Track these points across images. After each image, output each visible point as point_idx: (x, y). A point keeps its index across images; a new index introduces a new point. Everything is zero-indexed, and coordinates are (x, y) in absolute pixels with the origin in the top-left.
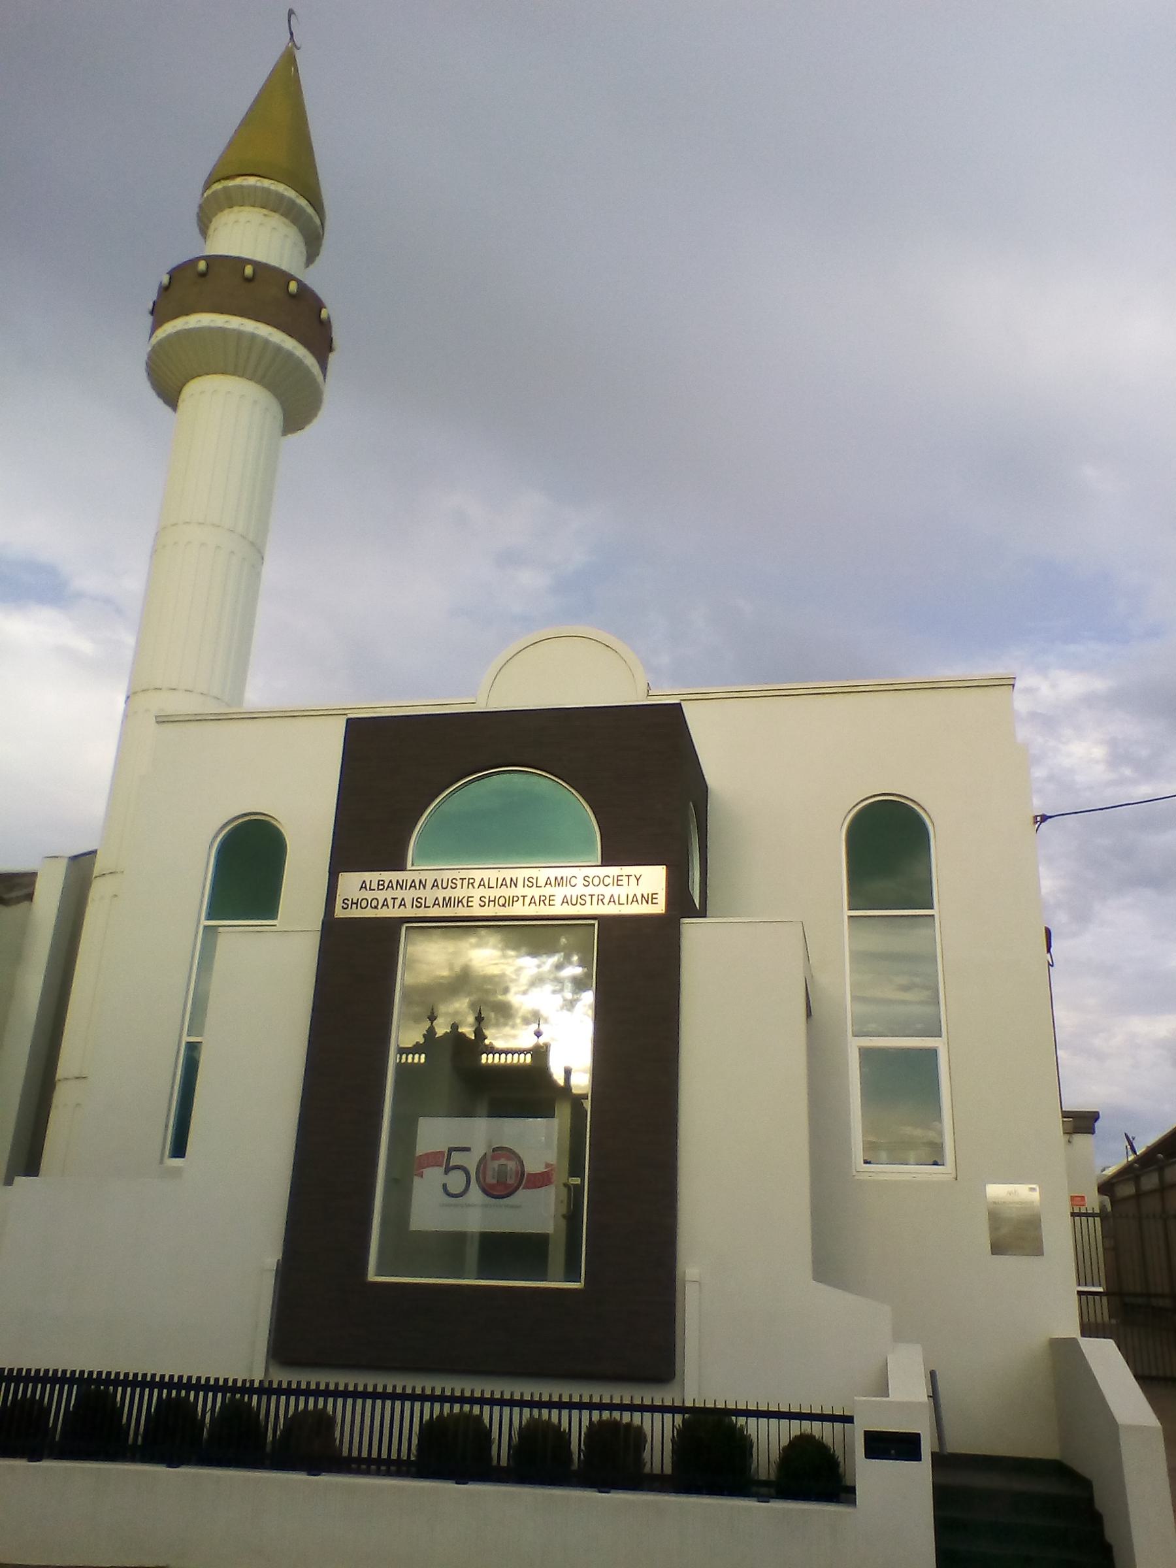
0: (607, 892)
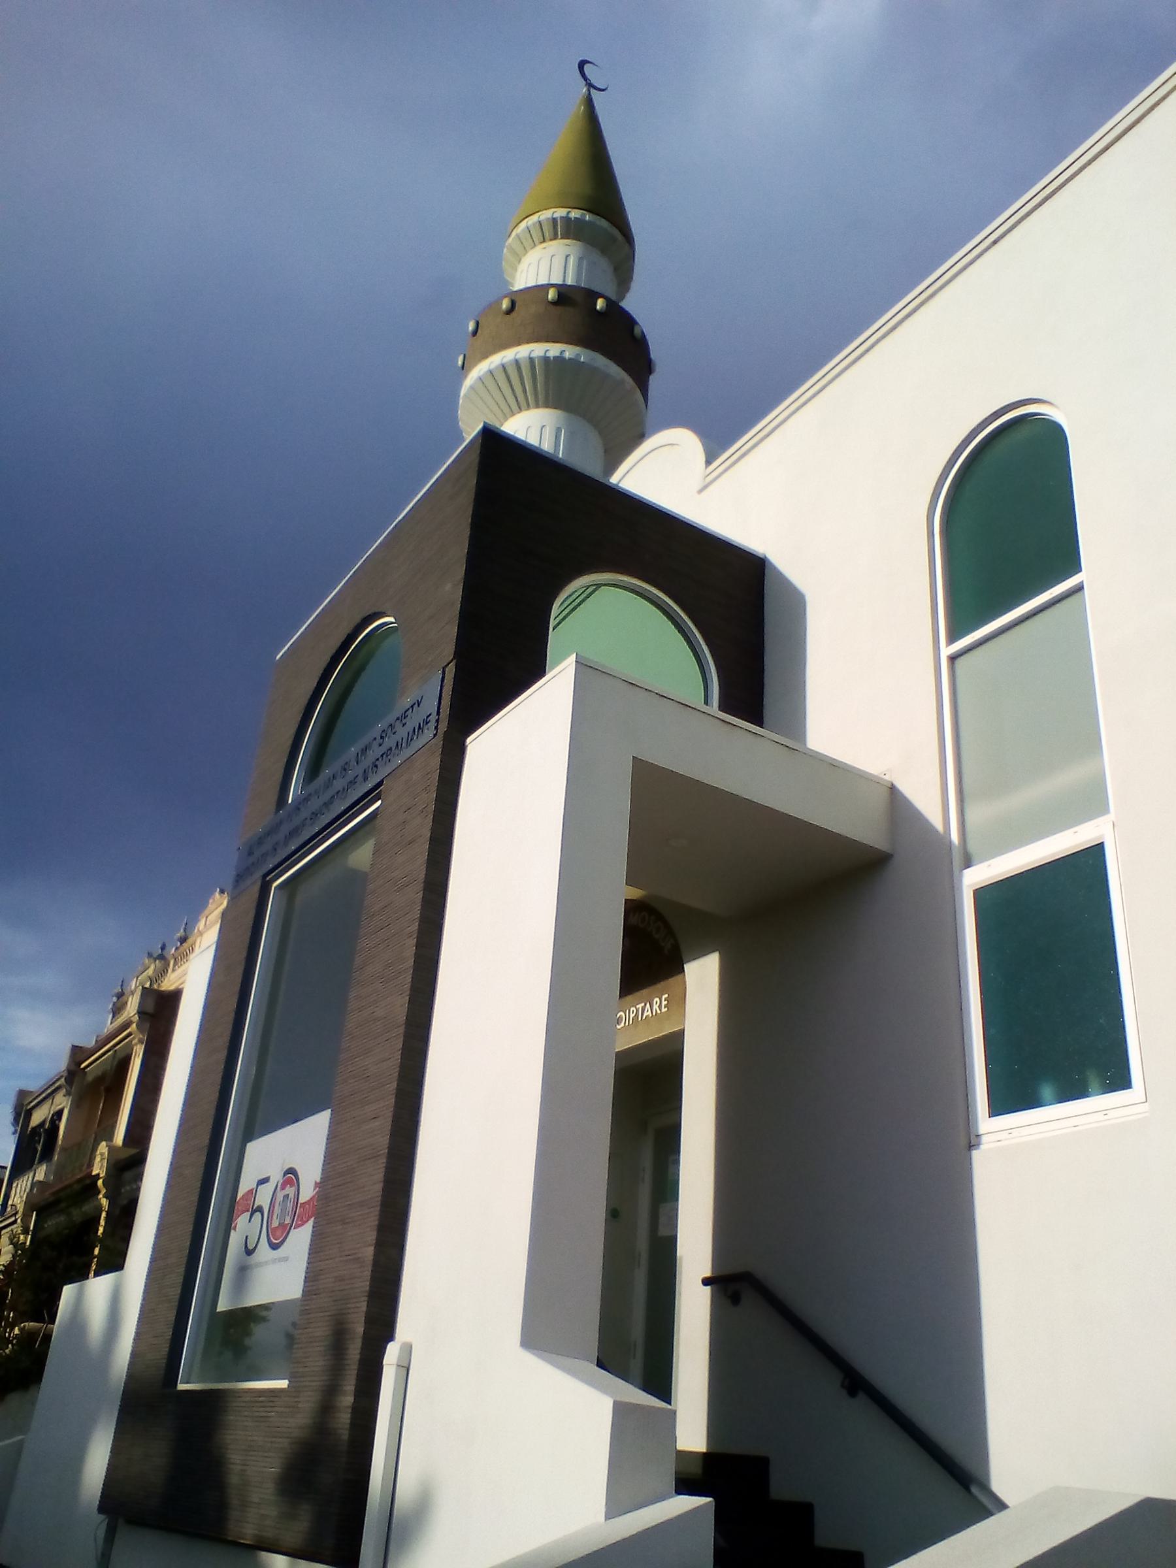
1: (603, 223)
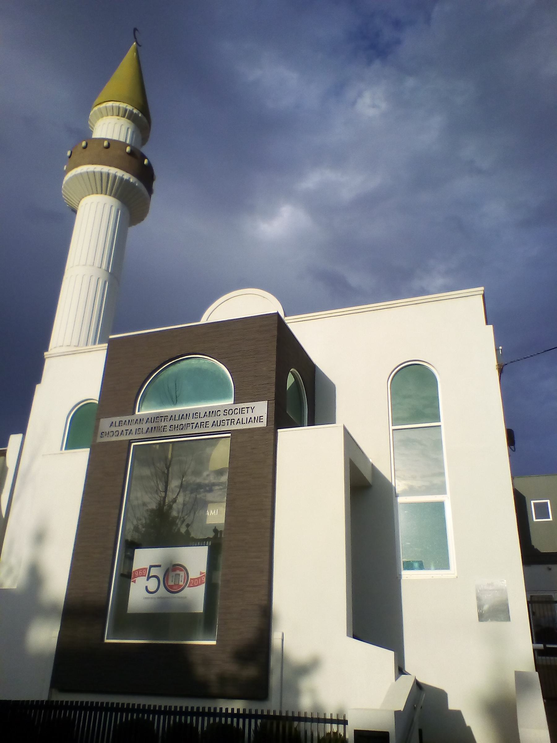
0: (236, 417)
1: (145, 120)
